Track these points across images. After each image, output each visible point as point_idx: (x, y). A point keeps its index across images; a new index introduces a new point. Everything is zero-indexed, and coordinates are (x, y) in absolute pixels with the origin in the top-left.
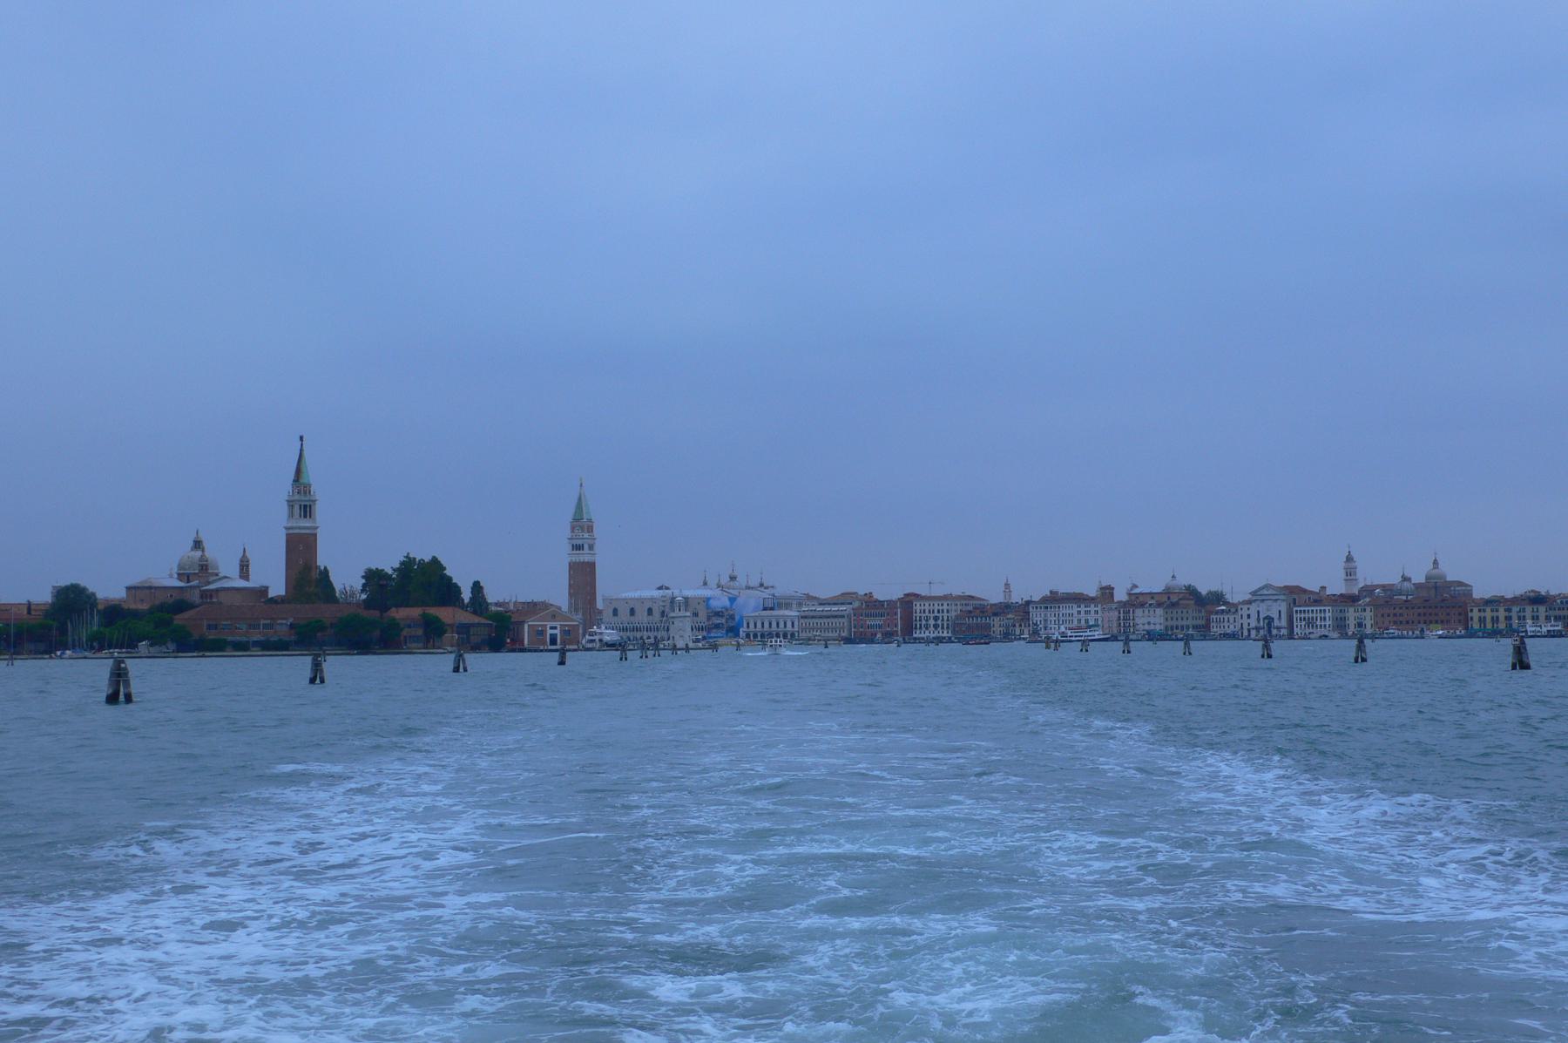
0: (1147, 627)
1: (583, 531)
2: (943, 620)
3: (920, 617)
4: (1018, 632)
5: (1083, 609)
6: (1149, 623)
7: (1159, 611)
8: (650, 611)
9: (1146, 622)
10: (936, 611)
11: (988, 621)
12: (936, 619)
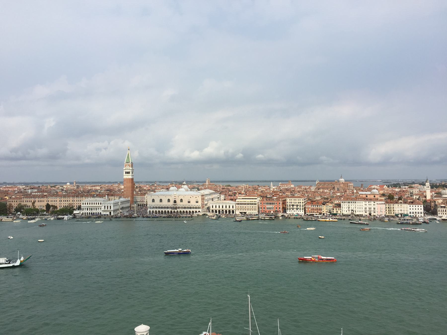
0: (400, 212)
1: (130, 167)
2: (300, 206)
3: (290, 205)
6: (401, 210)
8: (169, 200)
9: (400, 209)
10: (297, 203)
11: (313, 207)
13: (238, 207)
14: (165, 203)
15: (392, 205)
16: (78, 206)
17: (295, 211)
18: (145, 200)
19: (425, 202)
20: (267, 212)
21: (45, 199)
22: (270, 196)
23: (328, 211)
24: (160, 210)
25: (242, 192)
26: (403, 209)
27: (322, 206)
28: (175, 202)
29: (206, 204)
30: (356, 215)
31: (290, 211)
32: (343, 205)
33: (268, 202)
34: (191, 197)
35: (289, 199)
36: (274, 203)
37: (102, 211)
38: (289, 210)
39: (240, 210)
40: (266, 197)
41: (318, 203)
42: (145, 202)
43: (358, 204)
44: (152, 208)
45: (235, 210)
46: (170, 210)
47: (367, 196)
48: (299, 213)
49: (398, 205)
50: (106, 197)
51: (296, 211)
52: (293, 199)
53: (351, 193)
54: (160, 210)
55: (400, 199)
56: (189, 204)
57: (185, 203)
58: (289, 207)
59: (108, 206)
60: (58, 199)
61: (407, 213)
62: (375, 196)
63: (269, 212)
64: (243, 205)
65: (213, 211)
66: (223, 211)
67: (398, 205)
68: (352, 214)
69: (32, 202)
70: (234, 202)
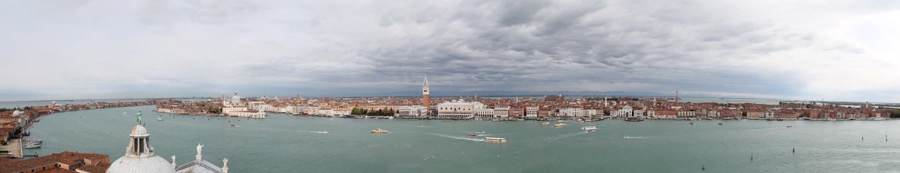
7: (595, 110)
8: (451, 109)
14: (449, 110)
19: (604, 108)
28: (455, 109)
41: (545, 109)
57: (461, 110)
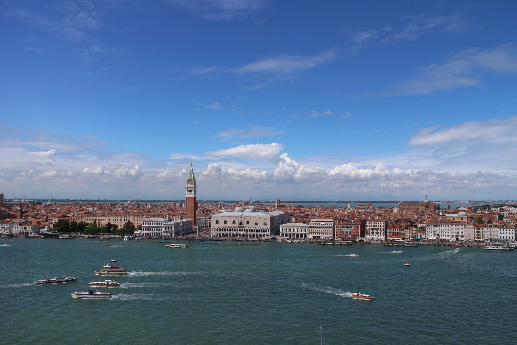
0: (489, 237)
2: (381, 230)
3: (369, 228)
4: (419, 237)
5: (382, 228)
6: (491, 235)
8: (234, 222)
10: (377, 226)
12: (377, 229)
13: (311, 230)
14: (230, 224)
15: (481, 229)
16: (138, 226)
17: (375, 236)
18: (209, 221)
20: (344, 236)
21: (106, 218)
22: (347, 219)
23: (411, 235)
24: (225, 232)
25: (316, 214)
26: (492, 233)
27: (405, 230)
28: (241, 224)
29: (276, 227)
30: (442, 240)
31: (369, 236)
32: (428, 229)
33: (344, 225)
34: (258, 219)
35: (368, 223)
36: (352, 226)
37: (163, 232)
38: (368, 235)
39: (314, 234)
40: (343, 220)
42: (209, 223)
43: (444, 228)
44: (216, 230)
45: (308, 234)
46: (235, 233)
47: (454, 219)
48: (379, 237)
49: (488, 229)
50: (168, 217)
51: (376, 236)
52: (373, 223)
53: (437, 215)
54: (225, 232)
55: (490, 222)
56: (256, 226)
57: (252, 225)
58: (368, 231)
59: (169, 227)
60: (119, 218)
61: (497, 238)
62: (462, 219)
63: (346, 236)
64: (317, 229)
65: (283, 234)
66: (294, 234)
67: (488, 229)
68: (437, 239)
69: (94, 220)
70: (307, 225)
